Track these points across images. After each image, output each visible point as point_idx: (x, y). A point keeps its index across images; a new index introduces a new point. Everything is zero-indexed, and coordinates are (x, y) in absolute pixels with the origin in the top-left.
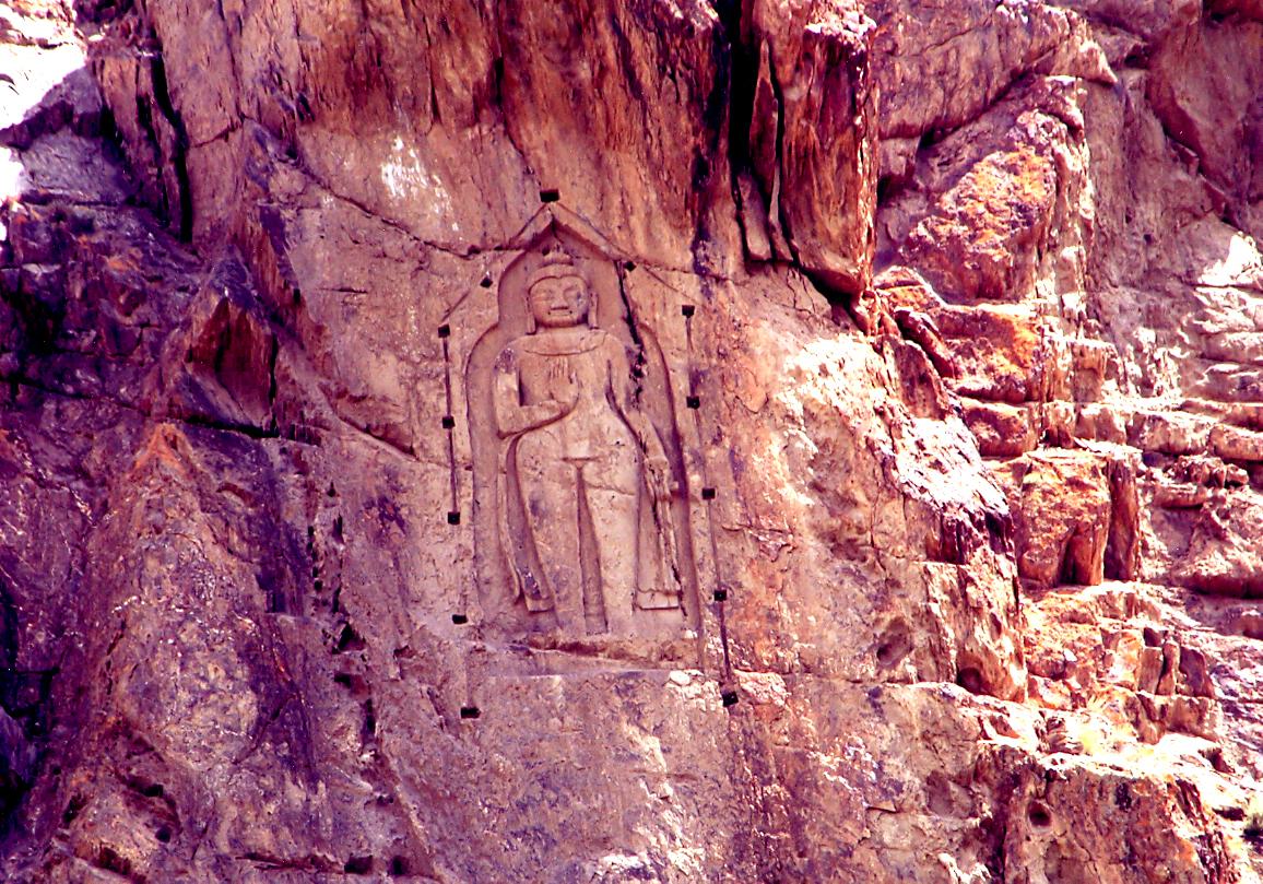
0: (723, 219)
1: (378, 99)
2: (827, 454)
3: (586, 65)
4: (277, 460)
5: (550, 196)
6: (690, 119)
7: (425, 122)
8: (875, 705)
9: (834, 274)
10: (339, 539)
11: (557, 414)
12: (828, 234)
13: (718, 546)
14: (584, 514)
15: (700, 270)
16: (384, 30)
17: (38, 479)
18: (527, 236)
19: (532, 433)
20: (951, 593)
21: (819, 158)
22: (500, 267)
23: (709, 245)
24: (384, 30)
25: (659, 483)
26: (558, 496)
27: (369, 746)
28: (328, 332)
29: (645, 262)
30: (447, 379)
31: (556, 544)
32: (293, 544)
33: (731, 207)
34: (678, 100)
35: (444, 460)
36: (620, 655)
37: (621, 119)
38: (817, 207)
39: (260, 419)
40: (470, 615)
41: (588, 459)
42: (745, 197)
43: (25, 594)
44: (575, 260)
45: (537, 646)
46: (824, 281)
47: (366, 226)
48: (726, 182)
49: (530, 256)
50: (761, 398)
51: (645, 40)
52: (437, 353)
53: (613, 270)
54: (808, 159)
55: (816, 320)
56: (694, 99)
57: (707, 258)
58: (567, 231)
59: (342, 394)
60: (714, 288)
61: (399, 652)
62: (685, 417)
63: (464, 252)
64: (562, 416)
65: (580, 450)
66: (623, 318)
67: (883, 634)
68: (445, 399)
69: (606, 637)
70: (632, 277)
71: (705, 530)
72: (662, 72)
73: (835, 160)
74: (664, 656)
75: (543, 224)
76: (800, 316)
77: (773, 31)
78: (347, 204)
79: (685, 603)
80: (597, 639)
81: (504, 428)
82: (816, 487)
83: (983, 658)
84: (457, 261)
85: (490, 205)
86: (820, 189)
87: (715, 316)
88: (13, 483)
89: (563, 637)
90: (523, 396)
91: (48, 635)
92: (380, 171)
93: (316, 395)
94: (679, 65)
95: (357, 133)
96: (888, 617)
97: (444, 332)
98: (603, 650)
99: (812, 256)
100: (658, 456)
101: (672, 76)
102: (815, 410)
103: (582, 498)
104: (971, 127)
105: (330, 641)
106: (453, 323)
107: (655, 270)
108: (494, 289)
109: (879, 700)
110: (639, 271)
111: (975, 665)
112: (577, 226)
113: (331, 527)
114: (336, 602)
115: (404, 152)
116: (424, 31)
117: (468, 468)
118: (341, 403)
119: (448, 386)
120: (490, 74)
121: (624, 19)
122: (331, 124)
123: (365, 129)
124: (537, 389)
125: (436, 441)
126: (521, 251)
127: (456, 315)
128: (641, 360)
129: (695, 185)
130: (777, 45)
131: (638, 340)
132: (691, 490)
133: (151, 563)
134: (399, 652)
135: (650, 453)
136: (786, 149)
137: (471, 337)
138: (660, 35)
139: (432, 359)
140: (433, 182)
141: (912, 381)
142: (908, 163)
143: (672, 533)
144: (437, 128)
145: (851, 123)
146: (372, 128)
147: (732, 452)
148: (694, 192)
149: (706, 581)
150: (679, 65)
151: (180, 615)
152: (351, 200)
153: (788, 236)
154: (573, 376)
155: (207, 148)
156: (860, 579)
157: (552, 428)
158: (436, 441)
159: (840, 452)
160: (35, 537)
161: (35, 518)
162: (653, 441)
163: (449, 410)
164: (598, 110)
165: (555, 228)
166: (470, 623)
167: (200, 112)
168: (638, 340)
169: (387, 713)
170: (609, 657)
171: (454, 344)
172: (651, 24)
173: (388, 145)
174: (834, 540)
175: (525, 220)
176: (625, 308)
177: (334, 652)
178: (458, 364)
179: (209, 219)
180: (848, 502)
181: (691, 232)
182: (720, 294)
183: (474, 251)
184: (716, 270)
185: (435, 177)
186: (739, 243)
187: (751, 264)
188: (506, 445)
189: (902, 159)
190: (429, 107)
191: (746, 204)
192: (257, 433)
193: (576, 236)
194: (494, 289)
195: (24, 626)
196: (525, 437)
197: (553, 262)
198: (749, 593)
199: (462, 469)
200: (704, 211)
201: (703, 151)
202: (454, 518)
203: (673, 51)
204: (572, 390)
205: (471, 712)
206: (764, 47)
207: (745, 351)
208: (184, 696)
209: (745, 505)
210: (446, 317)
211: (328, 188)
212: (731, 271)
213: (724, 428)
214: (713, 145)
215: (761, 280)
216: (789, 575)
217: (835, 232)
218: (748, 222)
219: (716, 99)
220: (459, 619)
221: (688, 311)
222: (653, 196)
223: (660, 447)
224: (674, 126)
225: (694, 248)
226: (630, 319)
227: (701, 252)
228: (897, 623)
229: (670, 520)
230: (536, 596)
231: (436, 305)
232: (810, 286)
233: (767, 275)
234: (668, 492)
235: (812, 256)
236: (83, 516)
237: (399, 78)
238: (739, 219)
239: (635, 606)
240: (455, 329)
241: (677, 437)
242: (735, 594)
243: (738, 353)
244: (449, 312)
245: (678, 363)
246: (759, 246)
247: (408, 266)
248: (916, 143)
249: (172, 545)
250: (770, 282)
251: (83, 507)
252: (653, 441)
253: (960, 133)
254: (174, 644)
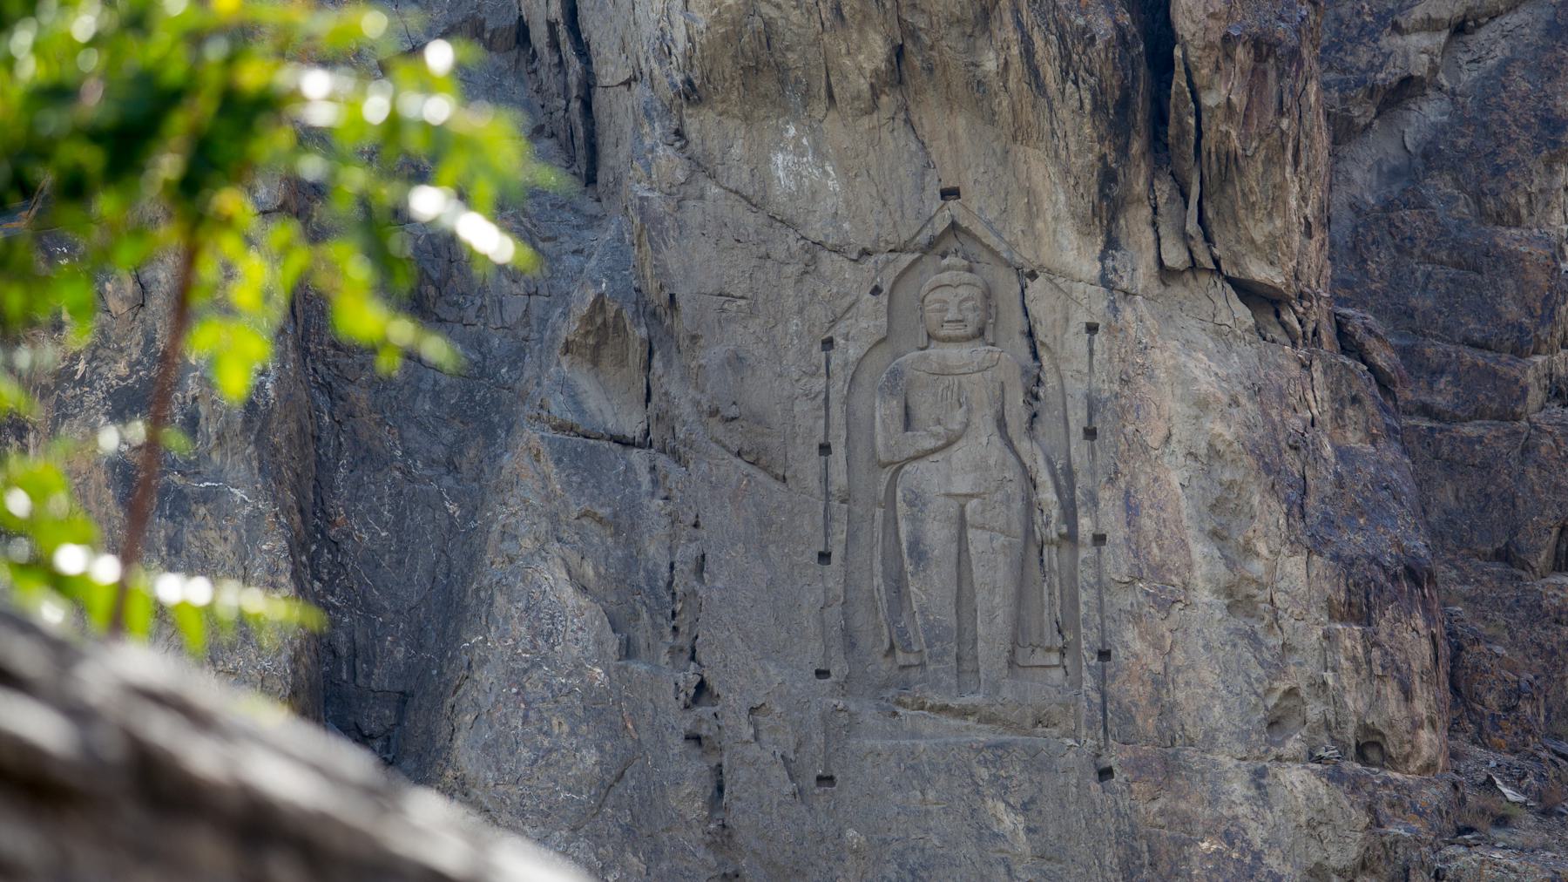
0: (1136, 223)
1: (768, 84)
2: (1233, 496)
3: (992, 55)
4: (645, 479)
5: (949, 193)
6: (1094, 127)
7: (819, 109)
8: (1259, 787)
9: (1260, 284)
10: (701, 580)
11: (940, 443)
12: (1252, 241)
13: (1106, 599)
14: (964, 557)
15: (1105, 281)
16: (774, 13)
17: (406, 472)
18: (923, 239)
19: (915, 464)
20: (1354, 659)
21: (1242, 163)
22: (890, 274)
23: (1118, 255)
24: (774, 13)
25: (1047, 524)
26: (938, 535)
27: (717, 815)
28: (702, 342)
29: (1049, 271)
30: (827, 399)
31: (930, 592)
32: (651, 577)
33: (1146, 212)
34: (1082, 107)
35: (817, 492)
36: (989, 719)
37: (1028, 115)
38: (1242, 212)
39: (632, 425)
40: (835, 670)
41: (972, 496)
42: (1162, 201)
43: (386, 604)
44: (975, 265)
45: (905, 705)
46: (1247, 291)
47: (751, 220)
48: (1140, 186)
49: (926, 259)
50: (1163, 433)
51: (1047, 42)
52: (818, 369)
53: (1014, 278)
54: (1230, 163)
55: (1236, 336)
56: (1098, 107)
57: (1115, 270)
58: (967, 232)
59: (714, 413)
60: (1121, 305)
61: (753, 710)
62: (1079, 450)
63: (854, 256)
64: (949, 444)
65: (962, 485)
66: (1022, 333)
67: (1276, 706)
68: (822, 422)
69: (978, 699)
70: (1036, 287)
71: (1092, 580)
72: (1065, 73)
73: (1259, 165)
74: (1038, 722)
75: (940, 225)
76: (1218, 333)
77: (1188, 37)
78: (733, 196)
79: (1067, 662)
80: (968, 700)
81: (883, 457)
82: (1216, 535)
83: (1386, 731)
84: (846, 264)
85: (885, 204)
86: (1244, 195)
87: (1121, 335)
88: (380, 476)
89: (936, 699)
90: (908, 421)
91: (407, 651)
92: (769, 160)
93: (685, 409)
94: (1082, 73)
95: (746, 118)
96: (1282, 686)
97: (828, 344)
98: (973, 714)
99: (1236, 264)
100: (1048, 495)
101: (1075, 82)
102: (1221, 447)
103: (962, 539)
104: (1507, 19)
105: (682, 696)
106: (837, 334)
107: (1060, 281)
108: (884, 299)
109: (1264, 781)
110: (1042, 278)
111: (1378, 738)
112: (979, 229)
113: (692, 566)
114: (694, 651)
115: (797, 139)
116: (816, 16)
117: (843, 502)
118: (713, 421)
119: (827, 409)
120: (889, 61)
121: (1027, 16)
122: (720, 107)
124: (922, 411)
125: (808, 466)
126: (917, 255)
127: (841, 327)
128: (1039, 381)
129: (1103, 195)
130: (1191, 50)
131: (1036, 356)
132: (1080, 537)
133: (500, 600)
134: (753, 710)
135: (1040, 489)
136: (1204, 154)
137: (853, 352)
138: (1062, 38)
139: (813, 375)
140: (825, 173)
141: (1342, 401)
142: (1432, 61)
143: (1057, 580)
144: (833, 115)
145: (1278, 125)
146: (762, 112)
147: (1127, 492)
148: (1100, 200)
149: (1088, 639)
150: (1082, 73)
151: (526, 660)
152: (736, 192)
153: (1208, 239)
154: (963, 400)
155: (611, 90)
156: (1253, 638)
157: (937, 457)
158: (808, 466)
159: (1246, 495)
160: (400, 541)
161: (400, 516)
162: (1044, 477)
163: (827, 435)
164: (1005, 104)
165: (954, 226)
166: (833, 678)
167: (605, 51)
168: (1036, 356)
169: (739, 781)
170: (979, 721)
171: (836, 358)
172: (1053, 27)
173: (781, 131)
174: (1230, 596)
176: (1025, 321)
177: (687, 707)
178: (839, 386)
179: (613, 168)
180: (1248, 550)
181: (1100, 241)
182: (1128, 314)
183: (865, 253)
184: (1124, 284)
185: (829, 169)
186: (1153, 252)
187: (1165, 273)
188: (885, 476)
189: (1425, 57)
190: (823, 93)
191: (1162, 210)
192: (625, 442)
193: (975, 238)
194: (884, 299)
195: (382, 640)
196: (907, 467)
197: (948, 268)
198: (1136, 656)
199: (836, 503)
200: (1113, 219)
201: (1110, 159)
202: (824, 557)
203: (1075, 57)
204: (959, 415)
205: (826, 780)
206: (1178, 52)
207: (1150, 377)
208: (525, 753)
209: (1137, 556)
211: (713, 176)
212: (1140, 286)
213: (1121, 466)
214: (1123, 151)
215: (1177, 290)
216: (1179, 634)
217: (1259, 239)
218: (1162, 231)
219: (1124, 104)
220: (822, 674)
221: (1092, 329)
222: (1062, 198)
223: (1050, 484)
224: (1076, 131)
225: (1102, 259)
226: (1030, 334)
227: (1109, 263)
228: (1291, 692)
229: (1055, 565)
230: (907, 649)
231: (818, 313)
232: (1234, 295)
233: (1185, 285)
234: (1054, 535)
235: (1236, 264)
236: (451, 516)
237: (790, 63)
238: (1154, 224)
239: (1011, 663)
240: (840, 341)
241: (1069, 472)
242: (1119, 654)
243: (1141, 380)
244: (834, 322)
245: (1077, 388)
246: (1175, 256)
247: (792, 270)
248: (1443, 37)
249: (523, 581)
250: (1187, 293)
251: (453, 508)
252: (1044, 477)
253: (1494, 24)
254: (518, 694)
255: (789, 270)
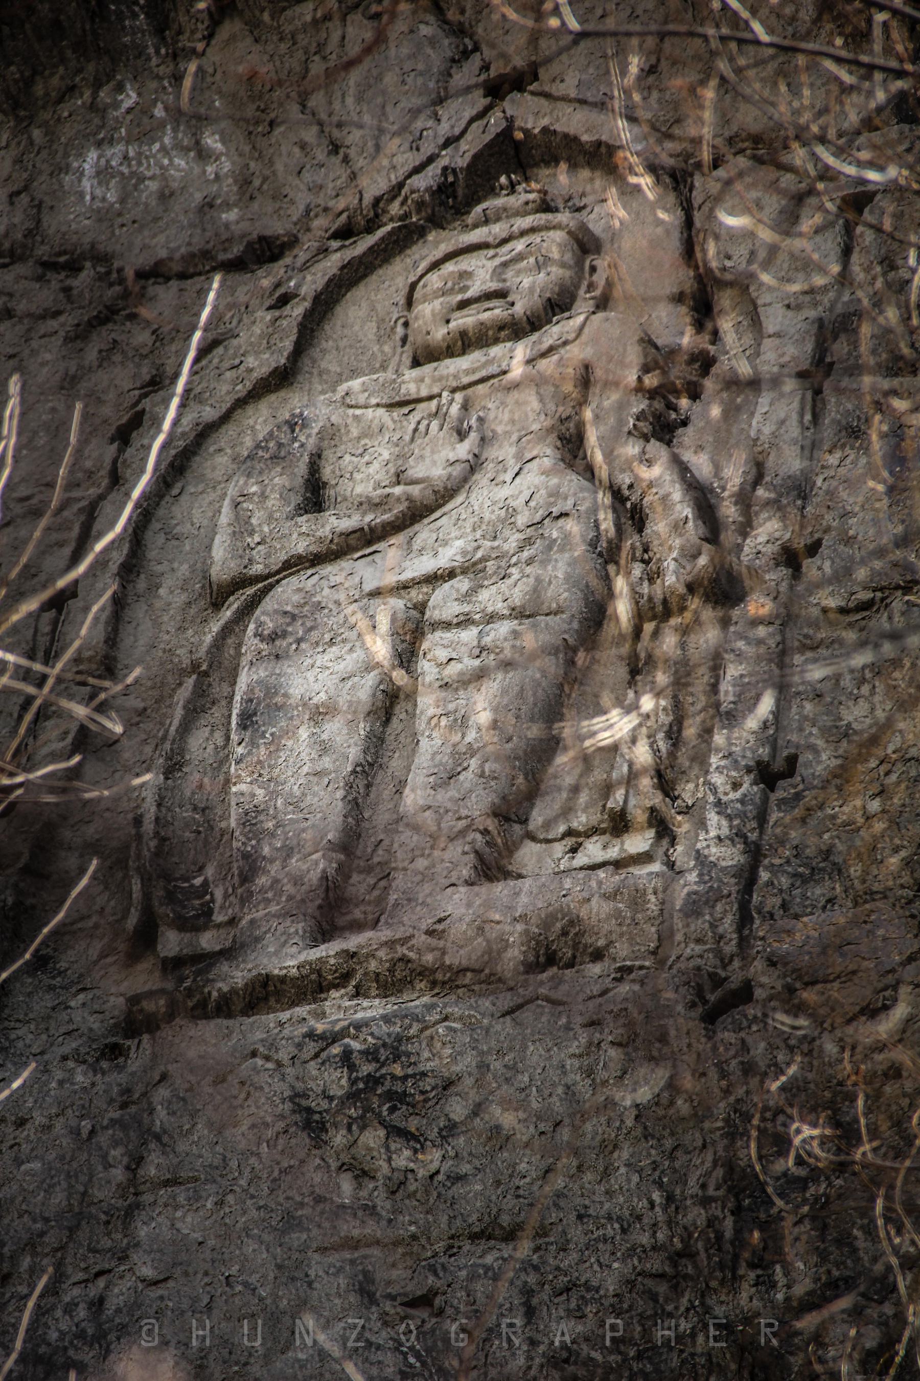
66: (679, 298)
108: (297, 310)
115: (142, 110)
123: (39, 90)
175: (428, 148)
185: (212, 142)
210: (146, 395)
255: (53, 324)
